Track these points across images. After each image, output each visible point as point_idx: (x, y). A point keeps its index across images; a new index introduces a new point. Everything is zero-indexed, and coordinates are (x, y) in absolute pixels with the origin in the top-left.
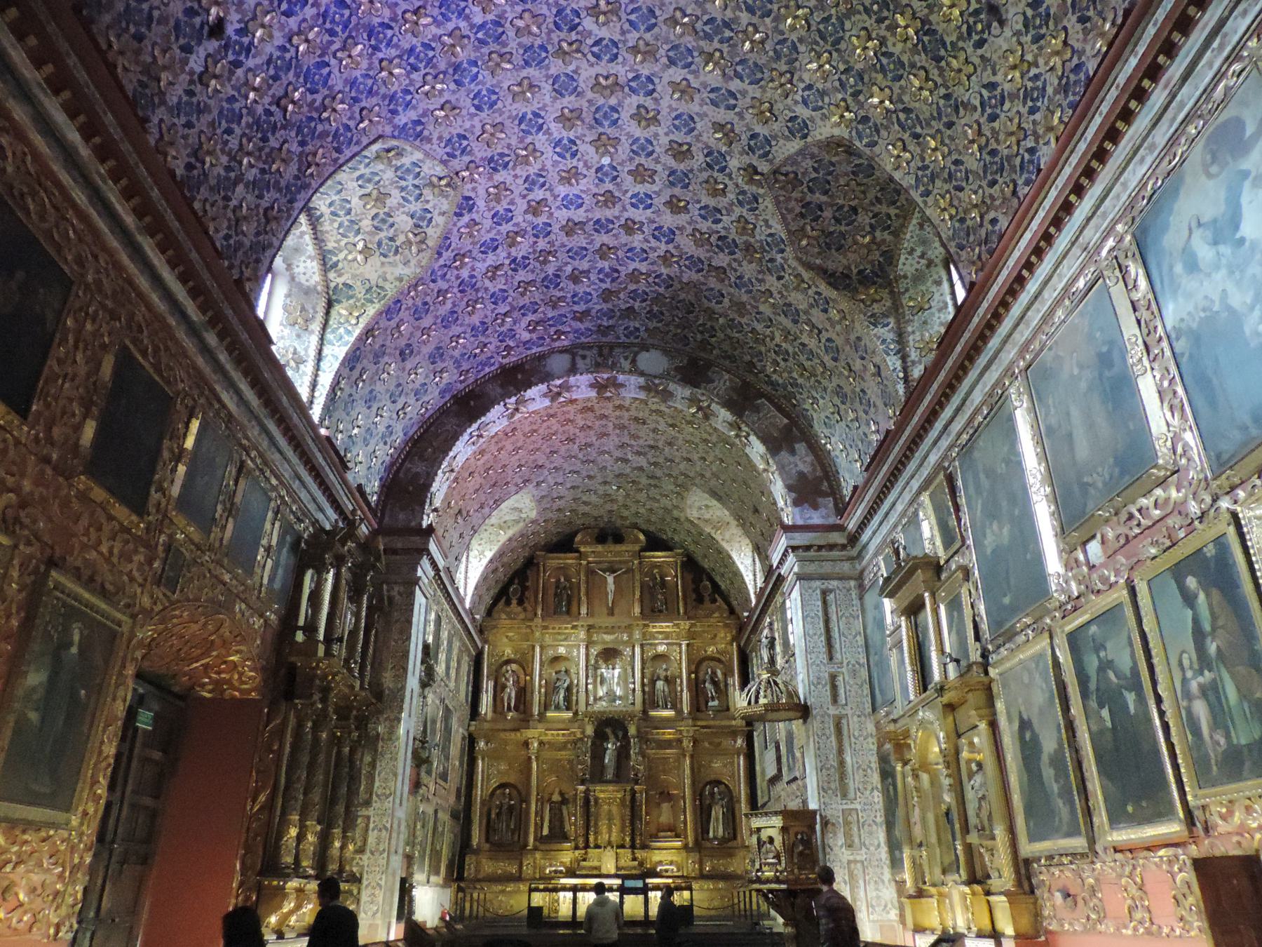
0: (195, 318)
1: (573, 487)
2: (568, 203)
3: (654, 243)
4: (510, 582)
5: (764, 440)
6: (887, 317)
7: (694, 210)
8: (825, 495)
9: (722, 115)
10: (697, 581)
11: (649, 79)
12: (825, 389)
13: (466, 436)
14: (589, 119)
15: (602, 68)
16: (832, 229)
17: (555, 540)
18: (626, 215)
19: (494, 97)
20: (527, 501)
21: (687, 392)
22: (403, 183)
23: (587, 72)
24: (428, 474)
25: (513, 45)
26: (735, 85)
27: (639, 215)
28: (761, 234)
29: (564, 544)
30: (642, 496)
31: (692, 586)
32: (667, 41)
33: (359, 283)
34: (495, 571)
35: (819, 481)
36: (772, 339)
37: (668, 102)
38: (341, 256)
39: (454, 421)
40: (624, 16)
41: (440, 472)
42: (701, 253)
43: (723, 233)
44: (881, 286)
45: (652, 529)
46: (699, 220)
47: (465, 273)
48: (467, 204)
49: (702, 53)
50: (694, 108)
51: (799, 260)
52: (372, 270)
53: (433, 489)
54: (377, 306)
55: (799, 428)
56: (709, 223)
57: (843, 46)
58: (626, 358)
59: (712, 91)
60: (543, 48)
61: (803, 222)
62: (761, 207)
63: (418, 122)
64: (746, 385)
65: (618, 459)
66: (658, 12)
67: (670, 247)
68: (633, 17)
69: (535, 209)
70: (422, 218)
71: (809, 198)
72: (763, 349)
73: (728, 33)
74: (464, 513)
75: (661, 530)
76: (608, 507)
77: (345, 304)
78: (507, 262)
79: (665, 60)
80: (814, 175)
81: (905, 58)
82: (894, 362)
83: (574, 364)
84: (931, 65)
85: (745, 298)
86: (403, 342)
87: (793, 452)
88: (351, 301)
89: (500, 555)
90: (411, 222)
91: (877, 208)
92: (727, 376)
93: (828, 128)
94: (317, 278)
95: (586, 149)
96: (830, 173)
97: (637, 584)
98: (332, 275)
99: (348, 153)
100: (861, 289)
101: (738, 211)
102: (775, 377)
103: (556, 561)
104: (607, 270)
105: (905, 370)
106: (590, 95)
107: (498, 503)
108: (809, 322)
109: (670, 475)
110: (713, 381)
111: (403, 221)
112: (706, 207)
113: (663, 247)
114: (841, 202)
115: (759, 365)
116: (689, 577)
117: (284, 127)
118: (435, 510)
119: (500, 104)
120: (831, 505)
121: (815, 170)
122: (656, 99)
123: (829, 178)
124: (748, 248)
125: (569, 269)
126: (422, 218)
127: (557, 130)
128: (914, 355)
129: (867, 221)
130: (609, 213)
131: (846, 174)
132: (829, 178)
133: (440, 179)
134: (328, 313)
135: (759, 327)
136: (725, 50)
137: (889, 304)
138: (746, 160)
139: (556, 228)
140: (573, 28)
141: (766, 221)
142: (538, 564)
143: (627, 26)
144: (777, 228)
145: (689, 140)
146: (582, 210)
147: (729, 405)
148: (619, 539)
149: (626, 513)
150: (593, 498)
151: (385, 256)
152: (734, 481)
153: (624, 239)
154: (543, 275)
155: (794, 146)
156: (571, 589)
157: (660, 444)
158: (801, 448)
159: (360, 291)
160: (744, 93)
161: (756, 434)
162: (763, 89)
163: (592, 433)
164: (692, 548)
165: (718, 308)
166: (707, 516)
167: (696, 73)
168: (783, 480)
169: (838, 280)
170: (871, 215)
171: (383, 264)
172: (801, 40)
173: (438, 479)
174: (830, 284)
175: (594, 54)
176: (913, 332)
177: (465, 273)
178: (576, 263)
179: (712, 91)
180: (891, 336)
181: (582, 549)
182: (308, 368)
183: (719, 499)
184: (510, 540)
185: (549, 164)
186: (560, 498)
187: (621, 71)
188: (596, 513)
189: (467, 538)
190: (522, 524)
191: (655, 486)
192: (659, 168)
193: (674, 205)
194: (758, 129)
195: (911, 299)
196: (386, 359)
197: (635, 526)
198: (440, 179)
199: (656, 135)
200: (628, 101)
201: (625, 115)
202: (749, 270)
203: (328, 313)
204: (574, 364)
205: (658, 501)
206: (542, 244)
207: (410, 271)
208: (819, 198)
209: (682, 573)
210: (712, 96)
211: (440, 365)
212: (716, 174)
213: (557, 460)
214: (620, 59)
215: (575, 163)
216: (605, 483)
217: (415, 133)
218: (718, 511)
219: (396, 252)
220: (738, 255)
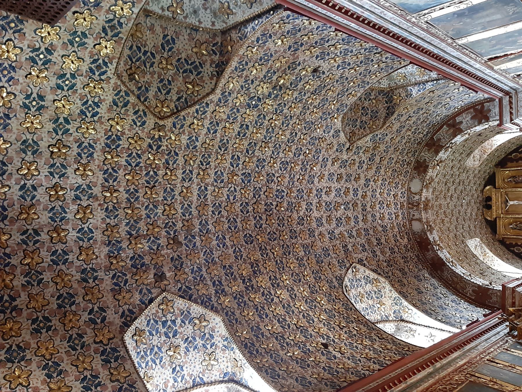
1: (464, 221)
2: (357, 222)
3: (370, 187)
4: (513, 252)
5: (455, 136)
6: (407, 90)
7: (359, 171)
8: (483, 107)
9: (329, 163)
10: (512, 160)
11: (317, 191)
12: (434, 112)
13: (453, 268)
14: (329, 213)
15: (314, 208)
16: (370, 116)
17: (490, 230)
18: (360, 198)
19: (325, 249)
20: (472, 242)
21: (431, 170)
22: (356, 286)
23: (316, 214)
24: (473, 286)
25: (309, 241)
26: (321, 159)
27: (360, 193)
28: (370, 144)
29: (492, 225)
30: (468, 188)
31: (515, 163)
32: (306, 185)
33: (393, 308)
34: (508, 259)
35: (476, 110)
36: (409, 136)
37: (324, 183)
38: (383, 314)
39: (446, 273)
40: (300, 201)
41: (472, 281)
42: (374, 169)
43: (368, 159)
44: (393, 94)
45: (483, 183)
46: (363, 169)
47: (385, 264)
48: (360, 262)
49: (310, 172)
50: (326, 173)
51: (381, 128)
52: (388, 302)
53: (481, 284)
54: (403, 301)
55: (449, 120)
56: (364, 165)
57: (313, 121)
58: (414, 197)
59: (322, 167)
61: (367, 128)
62: (360, 145)
63: (336, 278)
64: (427, 145)
65: (451, 200)
66: (298, 188)
67: (371, 180)
68: (300, 197)
69: (359, 235)
70: (367, 280)
72: (413, 139)
73: (305, 163)
74: (482, 272)
75: (484, 179)
76: (473, 204)
77: (403, 314)
78: (379, 247)
79: (312, 185)
80: (351, 125)
81: (321, 98)
82: (429, 86)
83: (417, 220)
84: (326, 88)
85: (392, 148)
86: (415, 292)
87: (461, 122)
88: (401, 311)
89: (499, 256)
90: (369, 284)
92: (423, 154)
93: (338, 123)
94: (392, 324)
95: (339, 214)
97: (514, 189)
98: (391, 319)
99: (351, 306)
100: (394, 102)
101: (361, 154)
102: (425, 133)
103: (501, 229)
104: (379, 206)
105: (432, 81)
107: (474, 256)
108: (405, 121)
109: (459, 175)
110: (425, 159)
111: (368, 288)
112: (358, 167)
113: (372, 183)
114: (360, 114)
115: (419, 140)
116: (509, 164)
117: (349, 328)
118: (491, 284)
119: (327, 247)
120: (488, 104)
124: (374, 149)
125: (379, 221)
126: (367, 280)
128: (426, 78)
129: (367, 102)
130: (360, 205)
133: (353, 271)
134: (407, 322)
135: (404, 141)
136: (310, 163)
137: (401, 90)
138: (344, 152)
139: (365, 227)
140: (303, 219)
141: (366, 142)
142: (503, 238)
143: (302, 199)
144: (368, 138)
145: (336, 175)
146: (359, 216)
147: (437, 152)
148: (489, 199)
149: (476, 195)
150: (469, 211)
151: (382, 296)
152: (464, 146)
153: (368, 199)
154: (382, 232)
155: (342, 134)
156: (516, 222)
157: (445, 181)
158: (458, 119)
159: (397, 308)
160: (324, 155)
161: (451, 140)
162: (323, 148)
163: (439, 211)
164: (494, 163)
165: (395, 160)
166: (478, 157)
167: (316, 173)
168: (475, 126)
169: (390, 112)
171: (385, 297)
172: (310, 136)
173: (475, 282)
174: (392, 114)
175: (310, 211)
176: (415, 79)
177: (385, 264)
178: (377, 218)
179: (322, 167)
180: (416, 88)
181: (495, 216)
182: (434, 332)
183: (472, 152)
184: (491, 251)
185: (344, 229)
186: (469, 227)
187: (315, 201)
188: (476, 210)
189: (493, 271)
190: (483, 245)
191: (463, 182)
192: (345, 186)
193: (357, 179)
194: (335, 149)
195: (400, 81)
196: (423, 300)
197: (482, 191)
198: (353, 271)
199: (334, 187)
201: (328, 199)
202: (382, 147)
203: (407, 322)
204: (417, 220)
205: (470, 180)
206: (371, 232)
207: (388, 287)
208: (358, 123)
209: (508, 168)
210: (323, 167)
211: (422, 277)
212: (348, 164)
213: (452, 227)
214: (311, 202)
215: (343, 219)
216: (462, 206)
217: (341, 280)
218: (477, 153)
219: (380, 291)
220: (376, 153)
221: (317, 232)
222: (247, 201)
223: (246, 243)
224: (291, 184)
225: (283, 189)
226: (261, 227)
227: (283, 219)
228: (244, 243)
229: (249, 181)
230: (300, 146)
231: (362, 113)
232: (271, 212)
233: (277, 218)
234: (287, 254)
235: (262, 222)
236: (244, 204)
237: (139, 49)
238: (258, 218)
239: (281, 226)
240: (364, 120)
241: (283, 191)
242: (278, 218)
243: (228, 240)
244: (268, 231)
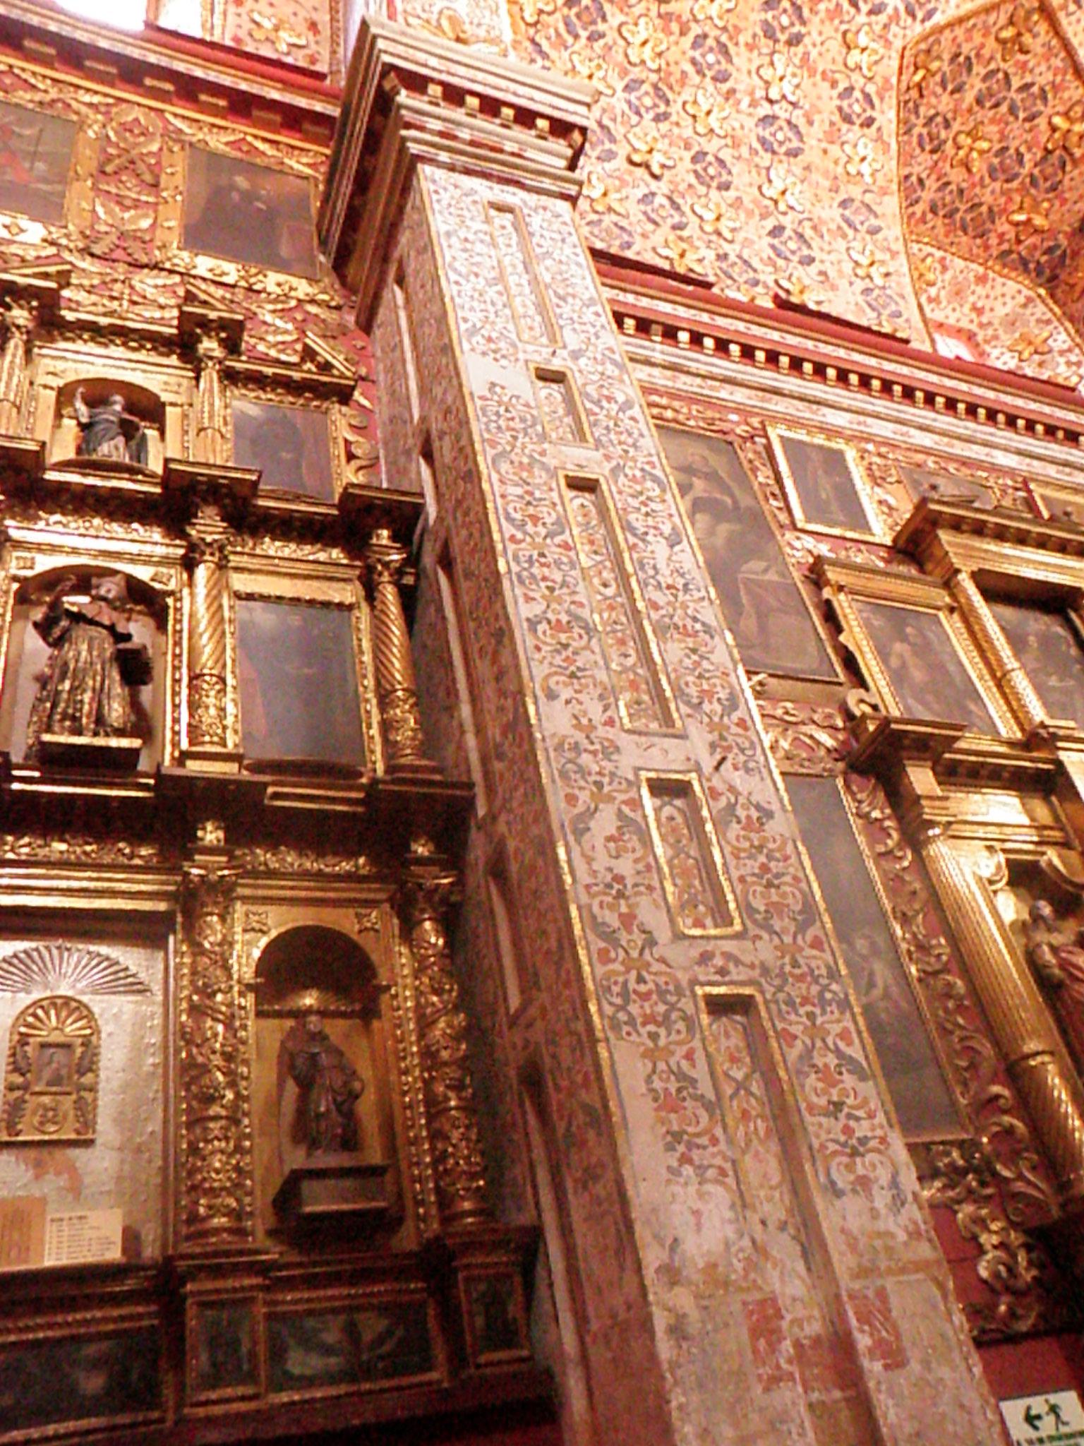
16: (922, 110)
71: (980, 70)
80: (1016, 83)
91: (931, 184)
96: (1012, 110)
114: (956, 126)
121: (1026, 87)
123: (1004, 108)
131: (1003, 137)
132: (1004, 108)
170: (924, 176)
231: (947, 125)
240: (945, 98)
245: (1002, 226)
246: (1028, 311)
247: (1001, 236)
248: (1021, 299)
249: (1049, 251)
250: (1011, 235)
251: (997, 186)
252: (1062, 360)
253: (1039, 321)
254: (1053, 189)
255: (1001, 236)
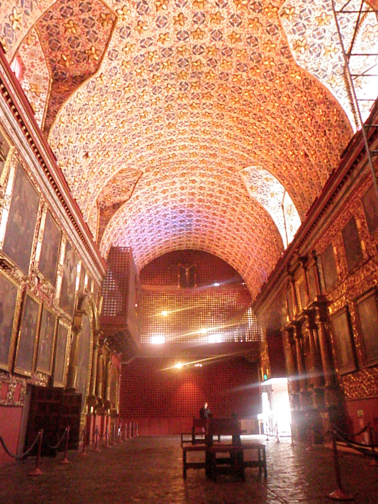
0: (350, 181)
11: (179, 39)
14: (208, 17)
19: (249, 40)
22: (306, 23)
23: (206, 40)
32: (173, 57)
40: (190, 64)
59: (152, 44)
60: (224, 54)
66: (178, 67)
68: (187, 63)
71: (90, 14)
79: (173, 49)
80: (94, 28)
91: (54, 21)
96: (88, 33)
106: (206, 30)
114: (73, 18)
119: (247, 36)
121: (95, 32)
122: (176, 30)
123: (87, 30)
127: (224, 12)
129: (54, 13)
132: (87, 30)
143: (189, 60)
170: (54, 17)
175: (203, 48)
179: (152, 44)
187: (192, 41)
200: (189, 27)
210: (151, 42)
214: (192, 47)
221: (228, 44)
222: (189, 114)
223: (222, 119)
224: (173, 76)
225: (179, 84)
226: (212, 105)
227: (207, 83)
228: (223, 120)
229: (173, 114)
230: (137, 86)
231: (71, 14)
232: (200, 95)
233: (206, 90)
234: (240, 91)
235: (208, 104)
236: (192, 115)
237: (114, 193)
238: (204, 106)
239: (213, 87)
240: (78, 8)
241: (181, 83)
242: (206, 88)
243: (217, 130)
244: (216, 100)
245: (59, 54)
246: (44, 81)
247: (56, 56)
248: (45, 76)
249: (63, 73)
250: (59, 59)
251: (67, 44)
252: (39, 102)
253: (44, 86)
254: (78, 61)
255: (56, 56)
